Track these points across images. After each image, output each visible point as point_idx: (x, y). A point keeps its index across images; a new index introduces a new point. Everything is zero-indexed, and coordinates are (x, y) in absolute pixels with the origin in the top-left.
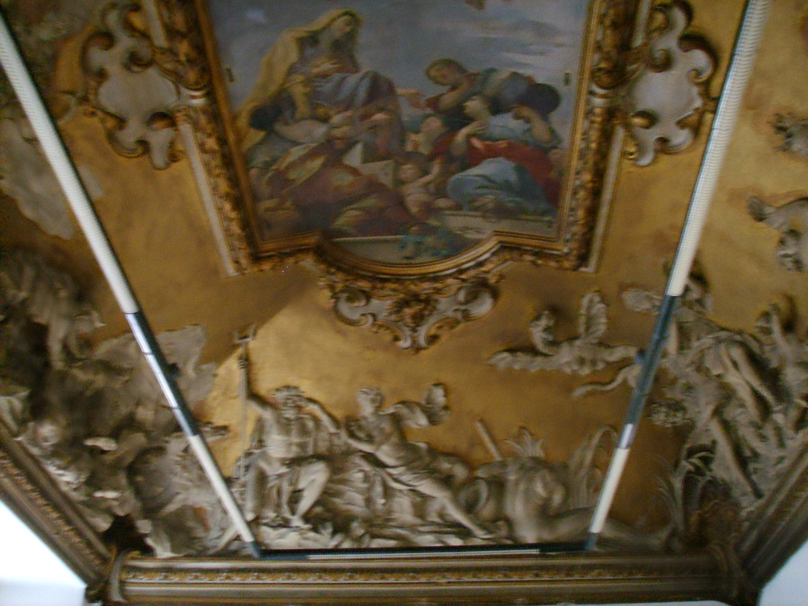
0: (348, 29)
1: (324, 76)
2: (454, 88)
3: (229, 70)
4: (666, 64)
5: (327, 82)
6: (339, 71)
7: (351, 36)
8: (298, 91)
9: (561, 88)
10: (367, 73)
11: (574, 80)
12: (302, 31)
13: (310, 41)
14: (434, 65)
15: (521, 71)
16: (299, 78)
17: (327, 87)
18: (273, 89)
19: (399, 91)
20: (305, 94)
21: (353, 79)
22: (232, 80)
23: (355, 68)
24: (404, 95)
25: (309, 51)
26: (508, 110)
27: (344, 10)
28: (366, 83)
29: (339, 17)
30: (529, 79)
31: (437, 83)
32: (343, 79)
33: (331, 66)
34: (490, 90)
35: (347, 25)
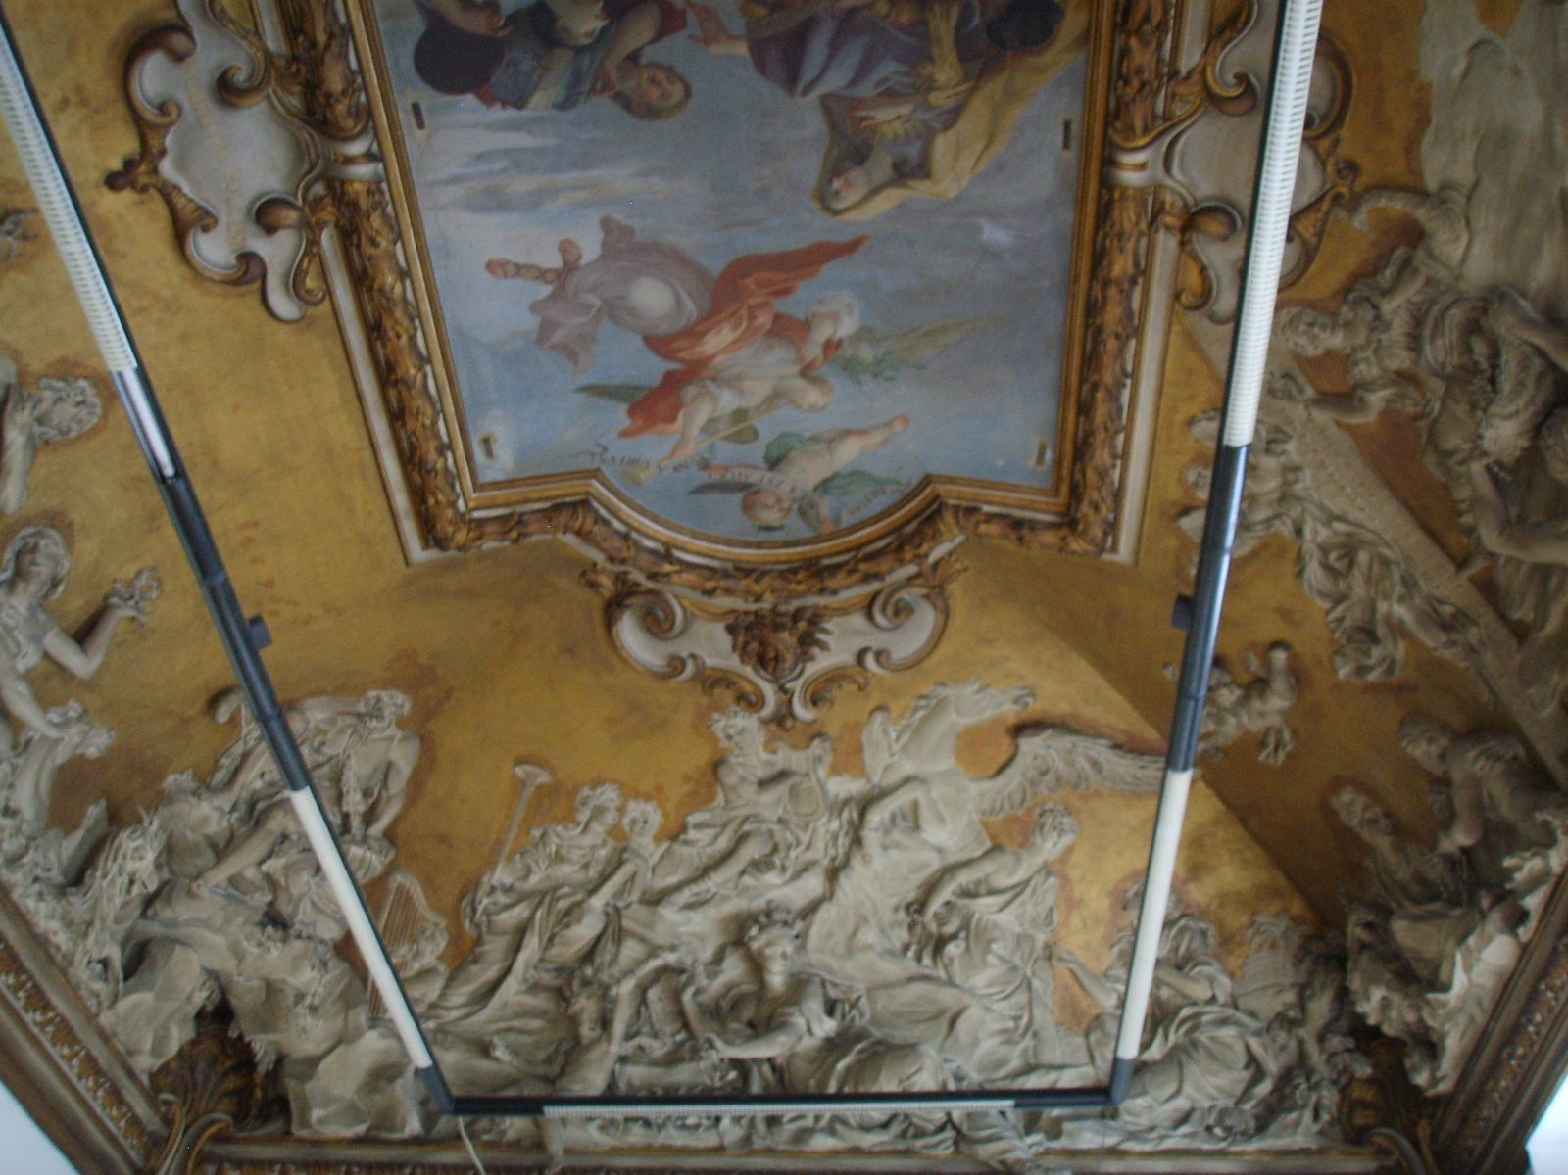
0: (836, 184)
1: (890, 95)
2: (634, 57)
3: (1066, 145)
4: (264, 215)
5: (885, 80)
6: (857, 103)
7: (834, 169)
8: (946, 72)
9: (427, 97)
10: (805, 92)
11: (405, 118)
12: (920, 190)
13: (910, 170)
14: (680, 106)
15: (511, 113)
16: (938, 98)
17: (888, 69)
18: (994, 87)
19: (741, 50)
20: (931, 60)
21: (836, 80)
22: (1067, 125)
23: (827, 103)
24: (733, 38)
25: (913, 151)
26: (512, 19)
27: (840, 218)
28: (808, 74)
29: (847, 209)
30: (488, 99)
31: (669, 70)
32: (853, 83)
33: (873, 113)
34: (562, 59)
35: (837, 193)
